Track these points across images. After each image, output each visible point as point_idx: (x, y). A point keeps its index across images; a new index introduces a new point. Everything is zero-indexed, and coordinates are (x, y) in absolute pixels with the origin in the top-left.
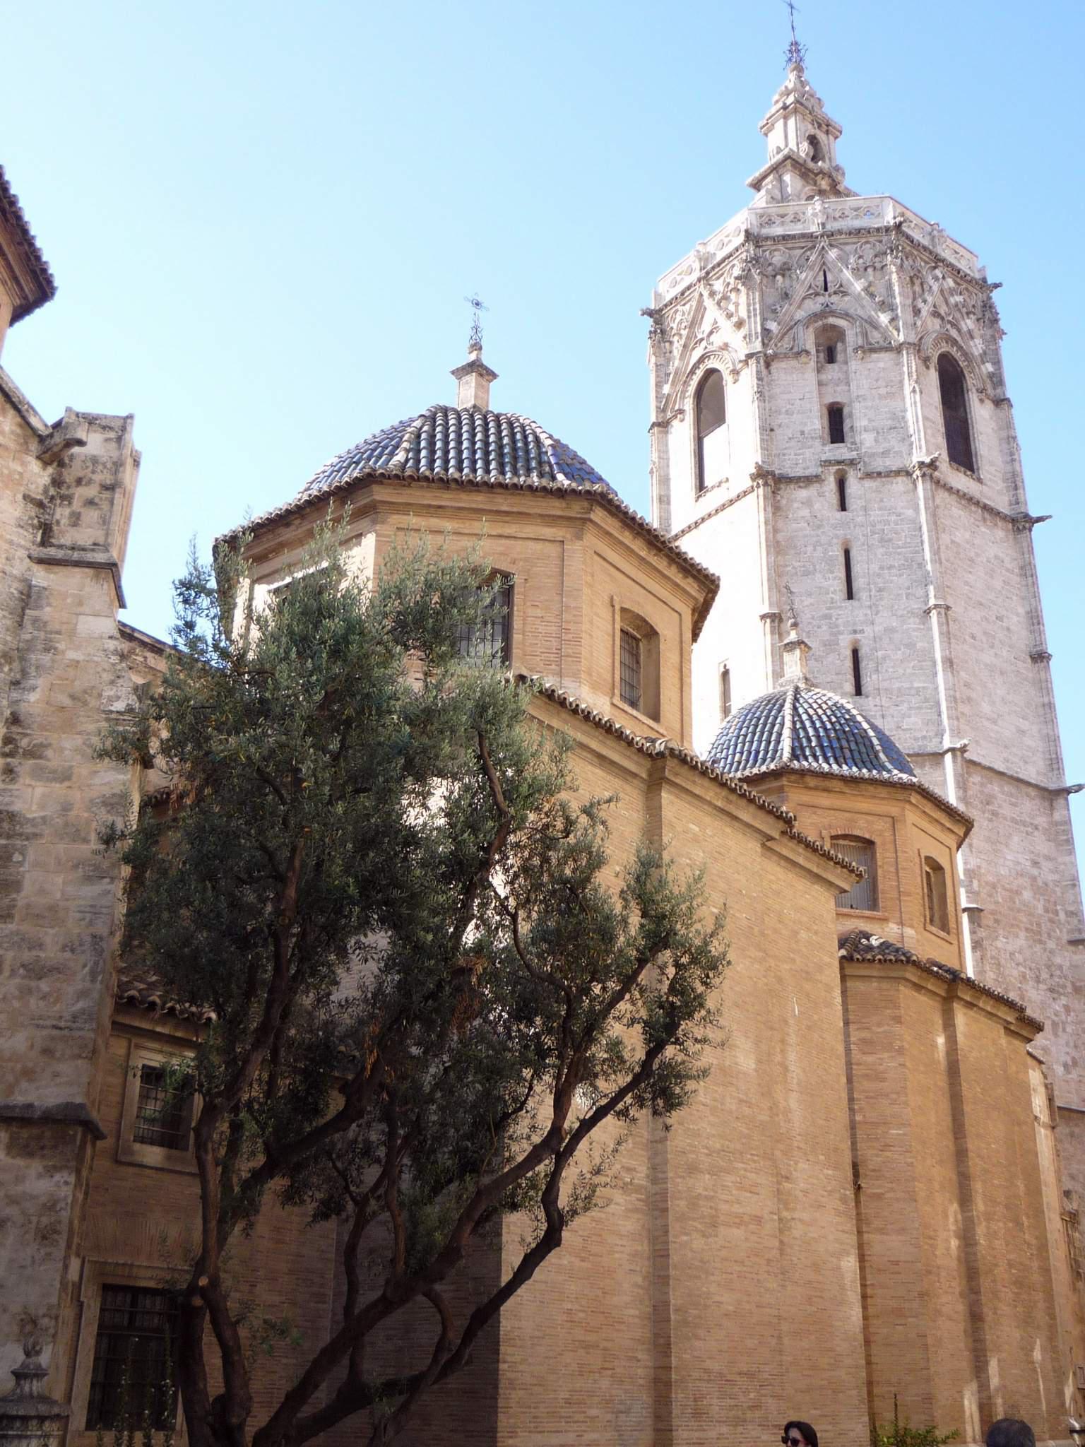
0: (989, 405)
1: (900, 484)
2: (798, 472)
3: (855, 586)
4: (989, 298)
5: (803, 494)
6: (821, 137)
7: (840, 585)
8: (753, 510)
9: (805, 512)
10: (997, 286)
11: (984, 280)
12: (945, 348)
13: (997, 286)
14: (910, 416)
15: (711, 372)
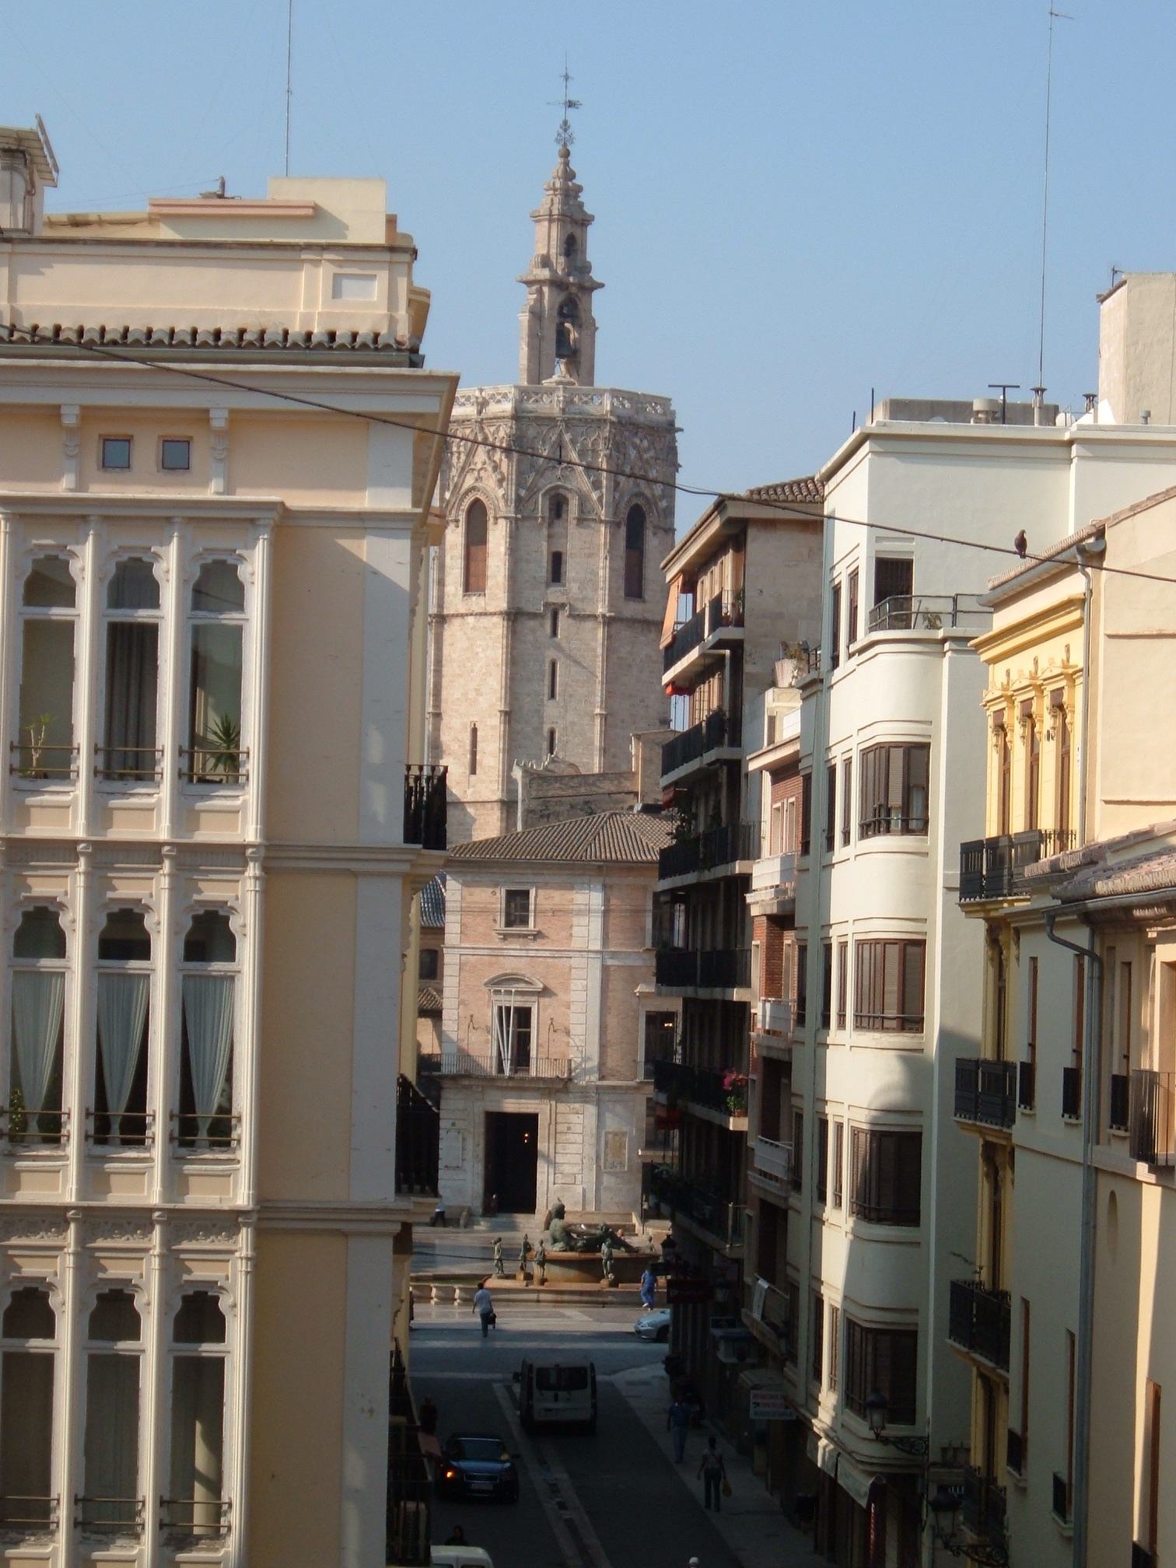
0: (661, 534)
1: (589, 624)
2: (531, 609)
3: (558, 689)
4: (674, 440)
5: (531, 623)
6: (578, 232)
7: (546, 691)
8: (498, 627)
9: (530, 638)
10: (681, 430)
11: (672, 424)
12: (635, 501)
13: (681, 430)
14: (601, 573)
15: (477, 501)
